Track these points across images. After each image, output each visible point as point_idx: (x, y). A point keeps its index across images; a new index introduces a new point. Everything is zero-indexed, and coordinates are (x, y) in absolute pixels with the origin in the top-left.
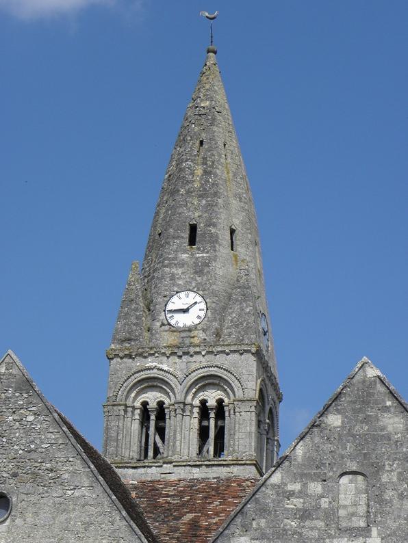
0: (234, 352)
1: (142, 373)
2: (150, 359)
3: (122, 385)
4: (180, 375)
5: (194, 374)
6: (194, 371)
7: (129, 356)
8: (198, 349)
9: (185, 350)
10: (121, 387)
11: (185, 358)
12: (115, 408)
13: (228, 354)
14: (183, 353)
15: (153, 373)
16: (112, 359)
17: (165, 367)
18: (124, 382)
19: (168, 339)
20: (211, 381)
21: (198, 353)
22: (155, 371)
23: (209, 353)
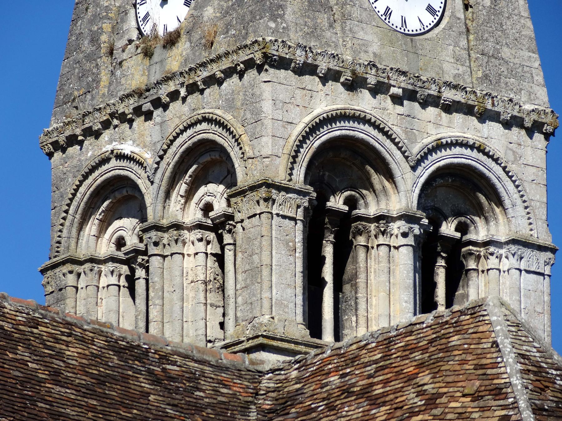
0: (229, 73)
1: (97, 173)
2: (106, 135)
3: (66, 212)
4: (148, 157)
5: (173, 149)
6: (172, 142)
7: (72, 140)
8: (172, 87)
9: (152, 95)
10: (64, 218)
11: (158, 113)
12: (57, 270)
13: (220, 82)
14: (152, 102)
15: (113, 168)
16: (50, 155)
17: (127, 148)
18: (69, 205)
19: (136, 73)
20: (206, 158)
21: (174, 96)
22: (114, 163)
23: (193, 89)
